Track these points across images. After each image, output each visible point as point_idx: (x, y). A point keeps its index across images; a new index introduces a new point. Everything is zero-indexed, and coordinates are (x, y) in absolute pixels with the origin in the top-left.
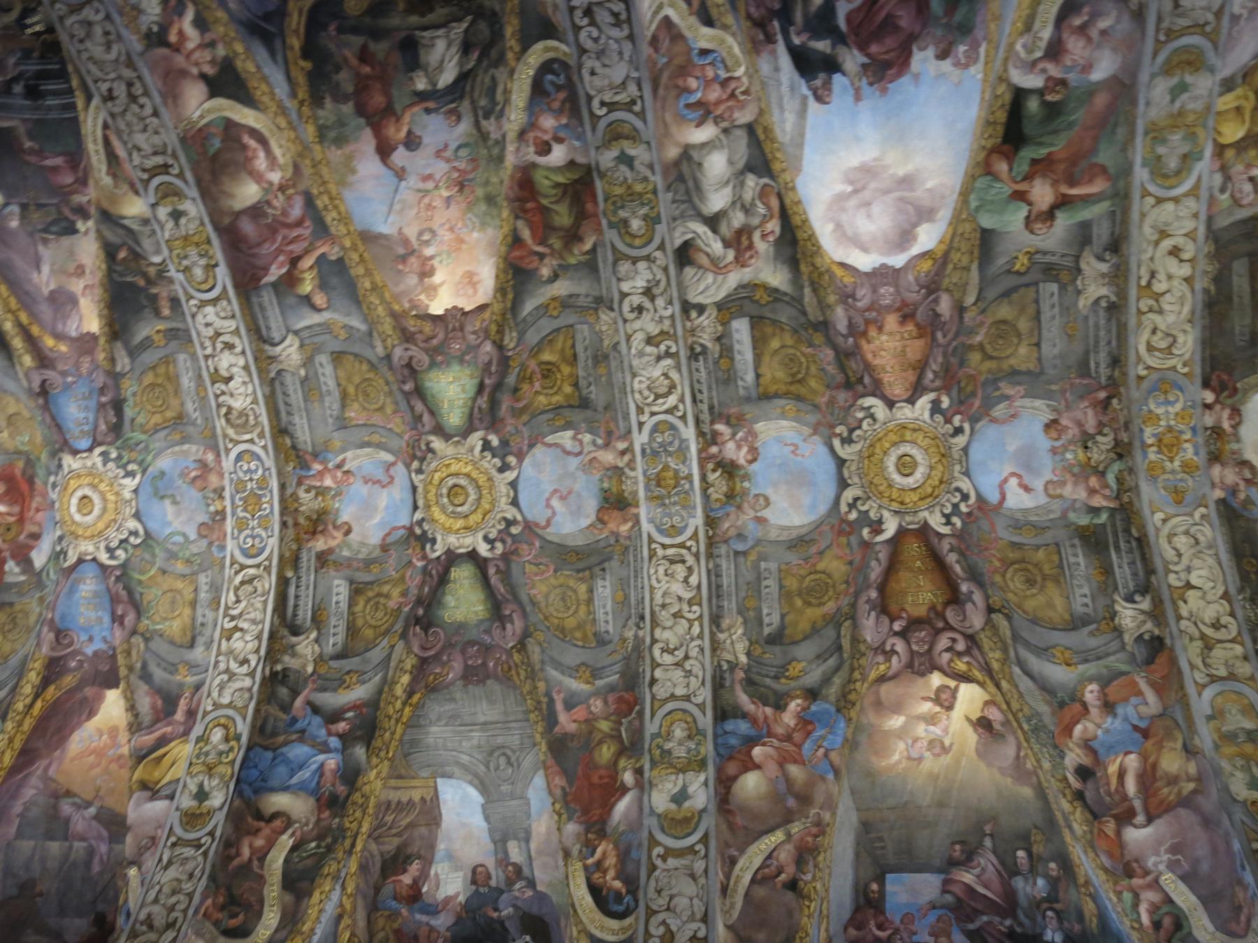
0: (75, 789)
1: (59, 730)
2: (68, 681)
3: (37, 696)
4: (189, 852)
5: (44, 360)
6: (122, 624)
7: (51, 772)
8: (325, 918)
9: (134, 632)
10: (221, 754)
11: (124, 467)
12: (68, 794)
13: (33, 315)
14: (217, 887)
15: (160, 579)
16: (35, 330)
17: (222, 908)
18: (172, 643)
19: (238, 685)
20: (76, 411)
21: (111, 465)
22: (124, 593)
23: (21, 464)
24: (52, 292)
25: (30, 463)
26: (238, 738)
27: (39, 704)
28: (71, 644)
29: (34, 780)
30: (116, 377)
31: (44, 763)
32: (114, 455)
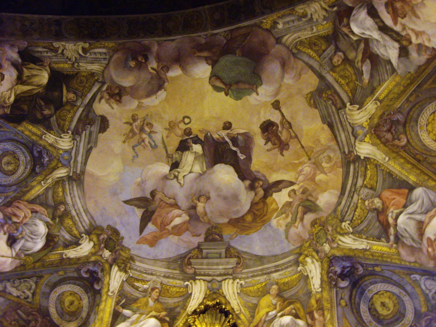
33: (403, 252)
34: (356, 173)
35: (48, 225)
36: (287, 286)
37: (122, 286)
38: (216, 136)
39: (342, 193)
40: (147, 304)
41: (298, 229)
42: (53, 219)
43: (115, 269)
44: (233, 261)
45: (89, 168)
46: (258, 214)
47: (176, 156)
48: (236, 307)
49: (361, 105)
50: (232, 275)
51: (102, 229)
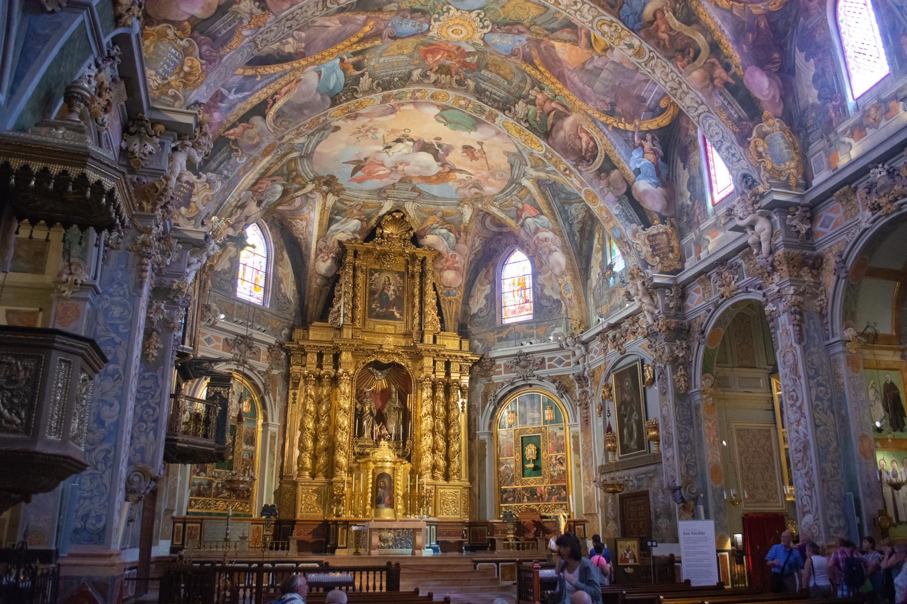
0: (583, 61)
1: (554, 61)
2: (534, 53)
3: (537, 68)
4: (653, 62)
5: (377, 35)
6: (522, 33)
7: (571, 68)
8: (713, 15)
9: (529, 28)
10: (615, 31)
11: (444, 12)
12: (584, 64)
13: (353, 34)
14: (674, 57)
15: (506, 10)
16: (361, 35)
17: (683, 57)
18: (541, 15)
19: (585, 10)
20: (408, 26)
21: (441, 18)
22: (508, 26)
23: (421, 47)
24: (341, 23)
25: (423, 44)
26: (613, 22)
27: (540, 68)
28: (519, 49)
29: (572, 76)
30: (400, 10)
31: (566, 70)
32: (437, 16)
33: (522, 232)
34: (514, 189)
35: (283, 185)
36: (448, 214)
37: (335, 203)
38: (426, 141)
39: (502, 191)
40: (352, 213)
41: (466, 191)
42: (288, 180)
43: (330, 195)
44: (416, 194)
45: (318, 149)
46: (440, 178)
47: (392, 144)
48: (412, 216)
49: (537, 171)
50: (414, 200)
51: (323, 177)
